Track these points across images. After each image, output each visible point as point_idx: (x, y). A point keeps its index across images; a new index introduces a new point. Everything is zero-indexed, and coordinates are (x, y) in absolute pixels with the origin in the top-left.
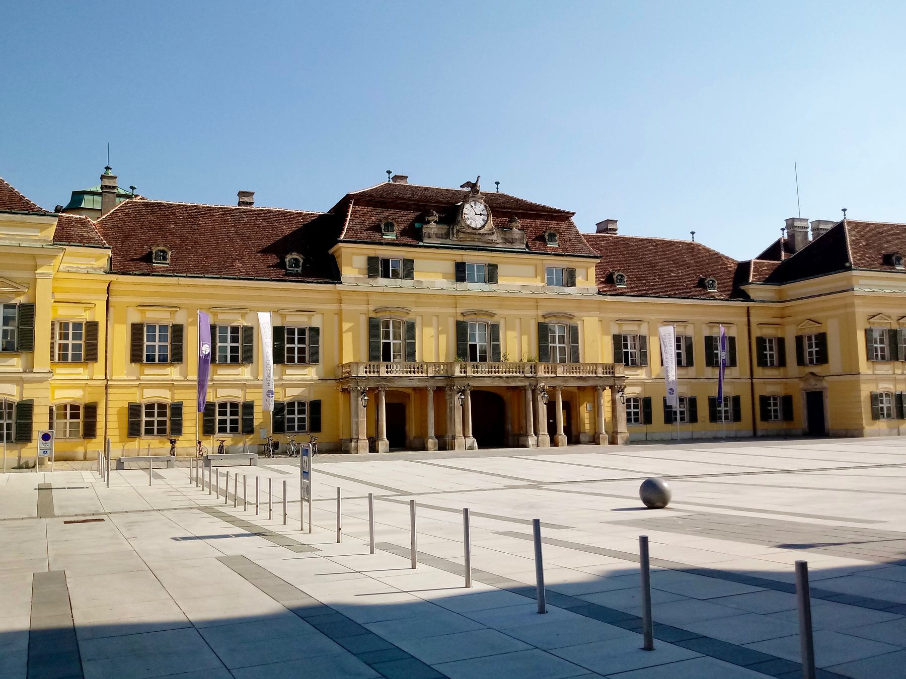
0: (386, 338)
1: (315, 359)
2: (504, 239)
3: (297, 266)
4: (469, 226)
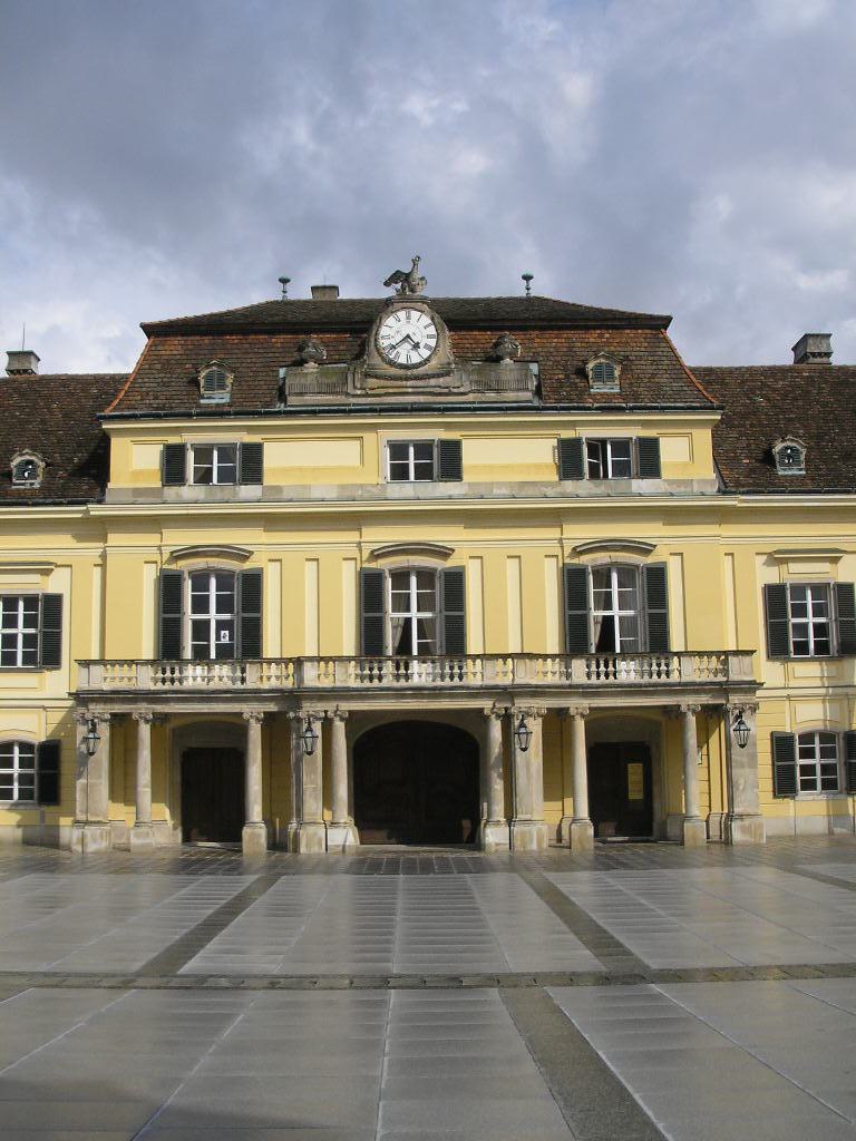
1: (51, 658)
3: (33, 475)
4: (392, 363)
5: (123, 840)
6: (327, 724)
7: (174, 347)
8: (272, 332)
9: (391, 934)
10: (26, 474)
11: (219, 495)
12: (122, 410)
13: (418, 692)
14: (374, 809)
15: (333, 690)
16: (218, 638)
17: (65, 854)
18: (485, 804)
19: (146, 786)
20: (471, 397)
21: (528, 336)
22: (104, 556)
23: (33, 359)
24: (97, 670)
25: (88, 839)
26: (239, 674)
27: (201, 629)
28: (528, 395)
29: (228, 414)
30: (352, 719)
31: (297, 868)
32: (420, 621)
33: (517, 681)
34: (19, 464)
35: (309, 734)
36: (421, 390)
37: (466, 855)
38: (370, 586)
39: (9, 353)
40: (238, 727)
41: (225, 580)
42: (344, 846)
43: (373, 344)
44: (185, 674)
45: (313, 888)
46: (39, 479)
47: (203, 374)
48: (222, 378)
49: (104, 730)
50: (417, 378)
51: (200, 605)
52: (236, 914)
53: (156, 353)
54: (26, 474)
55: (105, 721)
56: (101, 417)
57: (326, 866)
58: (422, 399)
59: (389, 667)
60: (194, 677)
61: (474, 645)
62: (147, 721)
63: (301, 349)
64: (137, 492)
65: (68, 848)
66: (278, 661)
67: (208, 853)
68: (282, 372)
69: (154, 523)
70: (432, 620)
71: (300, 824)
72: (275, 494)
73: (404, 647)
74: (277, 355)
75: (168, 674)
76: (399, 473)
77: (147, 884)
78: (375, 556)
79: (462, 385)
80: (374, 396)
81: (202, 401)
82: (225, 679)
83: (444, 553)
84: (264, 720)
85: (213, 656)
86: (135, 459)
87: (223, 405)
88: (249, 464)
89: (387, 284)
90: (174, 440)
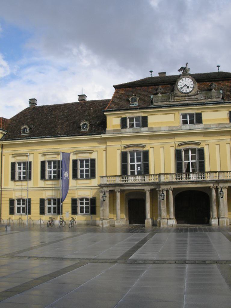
0: (136, 161)
2: (206, 96)
3: (86, 127)
4: (181, 92)
5: (113, 224)
6: (167, 191)
7: (122, 92)
8: (148, 86)
9: (186, 249)
10: (85, 127)
11: (136, 130)
12: (109, 109)
13: (192, 182)
14: (181, 215)
15: (169, 182)
16: (137, 169)
17: (98, 227)
18: (211, 213)
19: (119, 209)
20: (204, 101)
21: (219, 83)
22: (106, 148)
23: (85, 97)
24: (105, 179)
25: (104, 223)
26: (143, 179)
27: (133, 167)
28: (220, 99)
29: (138, 108)
30: (174, 190)
31: (160, 231)
32: (192, 163)
33: (219, 179)
34: (82, 125)
35: (162, 195)
36: (190, 99)
37: (206, 227)
38: (178, 154)
39: (79, 95)
40: (143, 193)
41: (138, 153)
42: (173, 225)
43: (176, 88)
44: (129, 179)
45: (164, 236)
46: (88, 128)
47: (130, 98)
48: (136, 99)
49: (107, 195)
50: (188, 96)
51: (132, 160)
52: (144, 243)
53: (118, 93)
54: (85, 127)
55: (108, 192)
56: (104, 111)
57: (168, 230)
58: (190, 102)
59: (184, 176)
60: (131, 180)
61: (207, 169)
62: (119, 192)
63: (157, 90)
64: (115, 131)
65: (98, 226)
66: (154, 175)
67: (136, 227)
68: (152, 97)
69: (119, 139)
70: (196, 163)
71: (161, 219)
72: (151, 129)
73: (188, 170)
74: (150, 92)
75: (124, 179)
76: (185, 122)
77: (119, 235)
78: (180, 145)
79: (201, 98)
80: (177, 101)
81: (131, 105)
82: (139, 180)
83: (198, 144)
84: (150, 191)
85: (136, 174)
86: (113, 121)
87: (136, 106)
88: (144, 122)
89: (179, 71)
90: (123, 116)
